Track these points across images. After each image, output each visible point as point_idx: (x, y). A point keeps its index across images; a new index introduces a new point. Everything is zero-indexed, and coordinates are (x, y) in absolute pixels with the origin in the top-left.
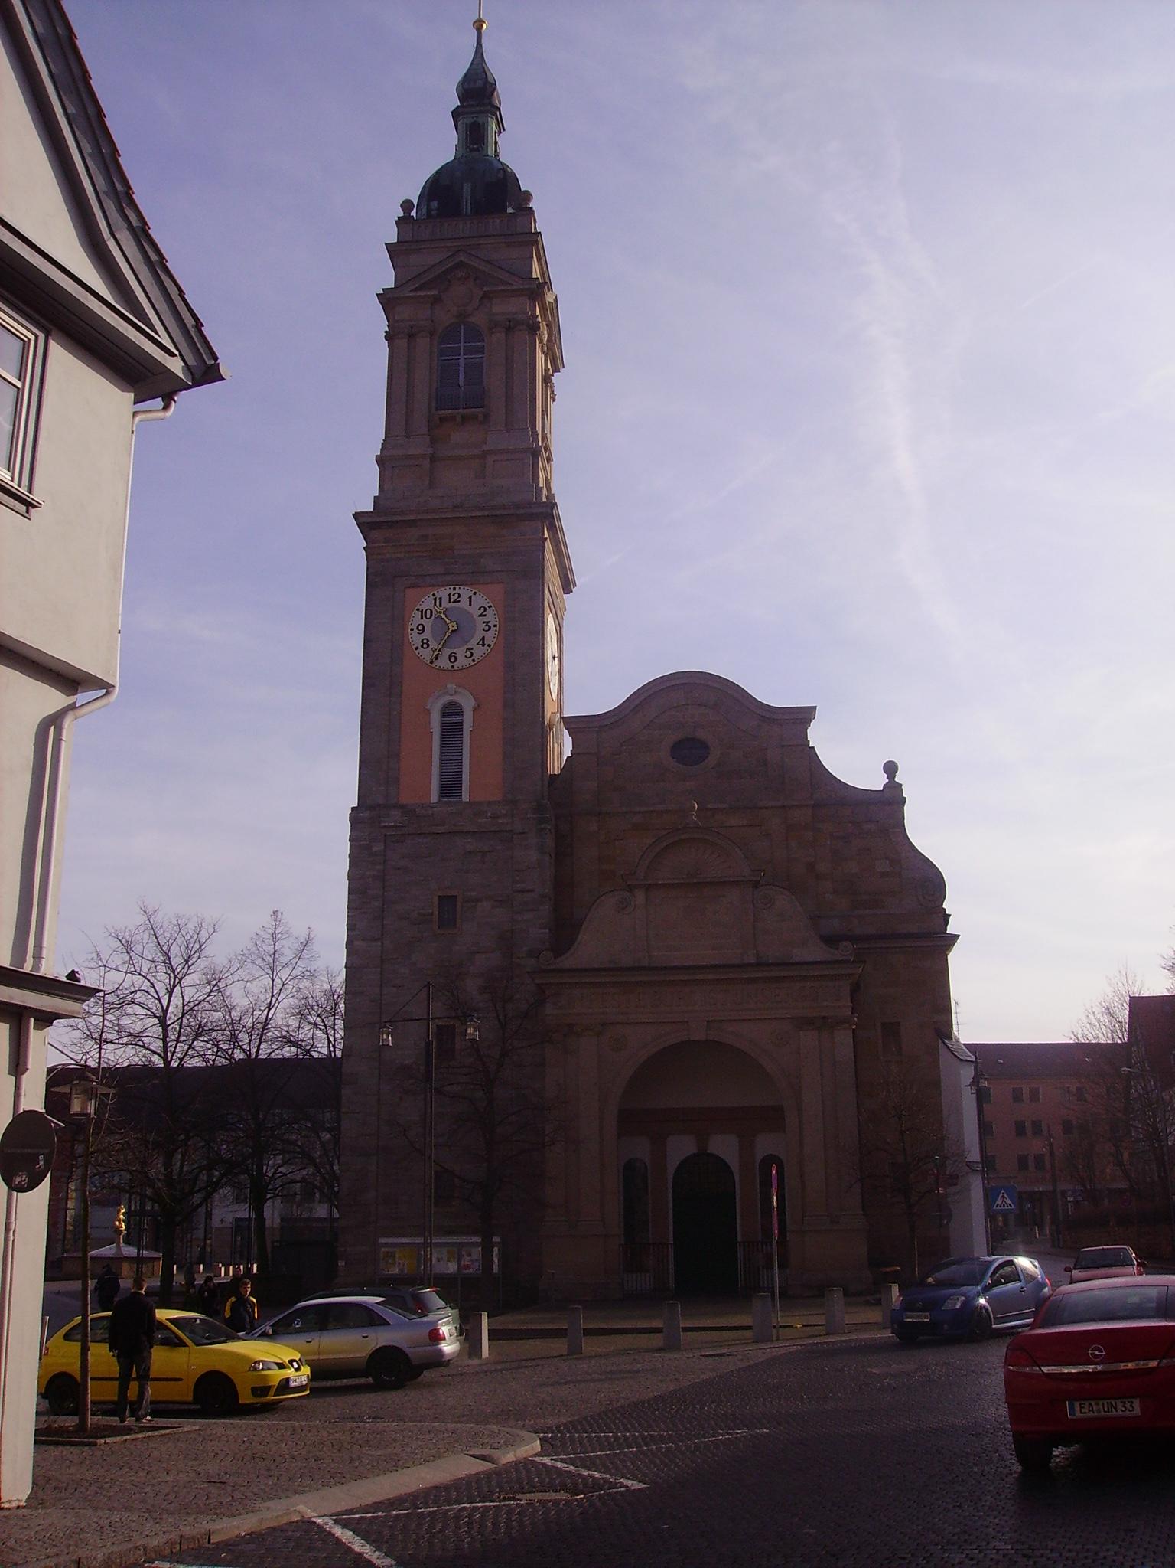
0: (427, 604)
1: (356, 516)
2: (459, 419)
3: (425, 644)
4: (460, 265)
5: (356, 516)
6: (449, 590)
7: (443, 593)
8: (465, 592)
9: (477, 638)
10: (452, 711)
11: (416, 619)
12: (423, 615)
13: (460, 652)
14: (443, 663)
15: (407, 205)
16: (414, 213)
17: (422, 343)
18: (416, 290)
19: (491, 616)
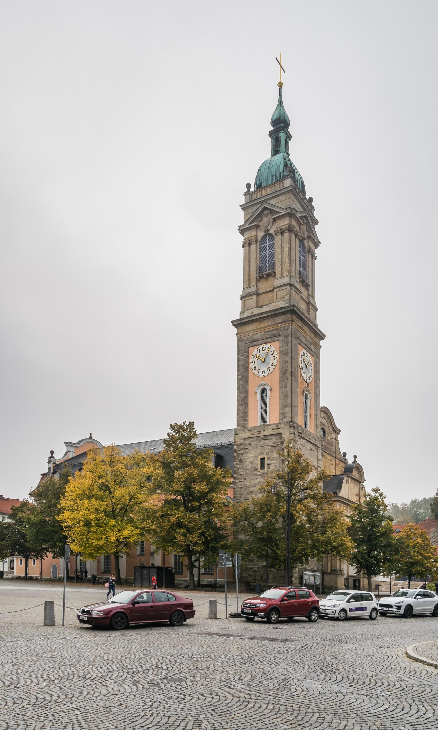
0: (255, 353)
1: (232, 322)
2: (265, 276)
3: (255, 368)
4: (265, 208)
5: (232, 322)
6: (262, 346)
7: (260, 347)
8: (267, 346)
9: (271, 364)
10: (264, 391)
11: (252, 359)
12: (254, 357)
13: (266, 369)
14: (261, 374)
15: (248, 186)
16: (252, 189)
17: (253, 246)
18: (249, 224)
19: (276, 354)
